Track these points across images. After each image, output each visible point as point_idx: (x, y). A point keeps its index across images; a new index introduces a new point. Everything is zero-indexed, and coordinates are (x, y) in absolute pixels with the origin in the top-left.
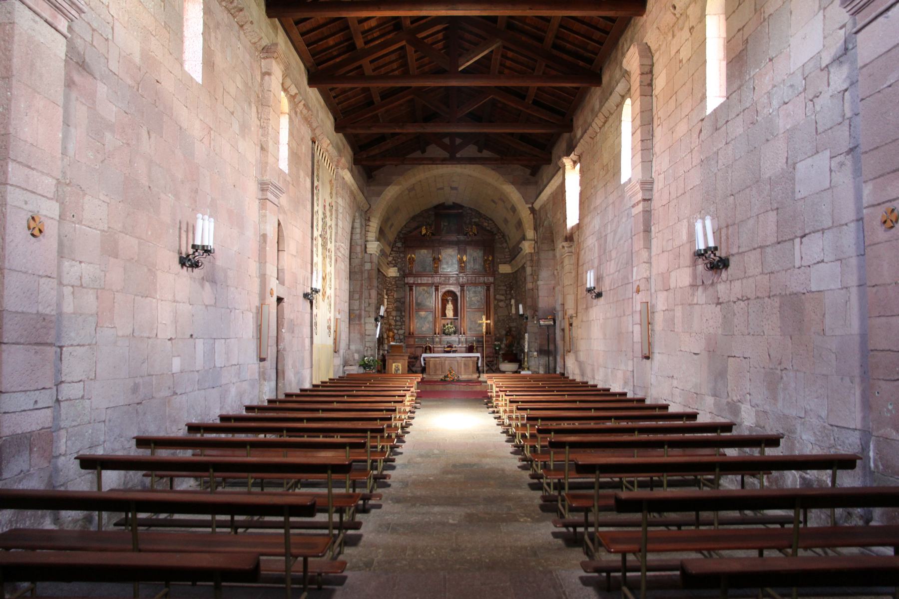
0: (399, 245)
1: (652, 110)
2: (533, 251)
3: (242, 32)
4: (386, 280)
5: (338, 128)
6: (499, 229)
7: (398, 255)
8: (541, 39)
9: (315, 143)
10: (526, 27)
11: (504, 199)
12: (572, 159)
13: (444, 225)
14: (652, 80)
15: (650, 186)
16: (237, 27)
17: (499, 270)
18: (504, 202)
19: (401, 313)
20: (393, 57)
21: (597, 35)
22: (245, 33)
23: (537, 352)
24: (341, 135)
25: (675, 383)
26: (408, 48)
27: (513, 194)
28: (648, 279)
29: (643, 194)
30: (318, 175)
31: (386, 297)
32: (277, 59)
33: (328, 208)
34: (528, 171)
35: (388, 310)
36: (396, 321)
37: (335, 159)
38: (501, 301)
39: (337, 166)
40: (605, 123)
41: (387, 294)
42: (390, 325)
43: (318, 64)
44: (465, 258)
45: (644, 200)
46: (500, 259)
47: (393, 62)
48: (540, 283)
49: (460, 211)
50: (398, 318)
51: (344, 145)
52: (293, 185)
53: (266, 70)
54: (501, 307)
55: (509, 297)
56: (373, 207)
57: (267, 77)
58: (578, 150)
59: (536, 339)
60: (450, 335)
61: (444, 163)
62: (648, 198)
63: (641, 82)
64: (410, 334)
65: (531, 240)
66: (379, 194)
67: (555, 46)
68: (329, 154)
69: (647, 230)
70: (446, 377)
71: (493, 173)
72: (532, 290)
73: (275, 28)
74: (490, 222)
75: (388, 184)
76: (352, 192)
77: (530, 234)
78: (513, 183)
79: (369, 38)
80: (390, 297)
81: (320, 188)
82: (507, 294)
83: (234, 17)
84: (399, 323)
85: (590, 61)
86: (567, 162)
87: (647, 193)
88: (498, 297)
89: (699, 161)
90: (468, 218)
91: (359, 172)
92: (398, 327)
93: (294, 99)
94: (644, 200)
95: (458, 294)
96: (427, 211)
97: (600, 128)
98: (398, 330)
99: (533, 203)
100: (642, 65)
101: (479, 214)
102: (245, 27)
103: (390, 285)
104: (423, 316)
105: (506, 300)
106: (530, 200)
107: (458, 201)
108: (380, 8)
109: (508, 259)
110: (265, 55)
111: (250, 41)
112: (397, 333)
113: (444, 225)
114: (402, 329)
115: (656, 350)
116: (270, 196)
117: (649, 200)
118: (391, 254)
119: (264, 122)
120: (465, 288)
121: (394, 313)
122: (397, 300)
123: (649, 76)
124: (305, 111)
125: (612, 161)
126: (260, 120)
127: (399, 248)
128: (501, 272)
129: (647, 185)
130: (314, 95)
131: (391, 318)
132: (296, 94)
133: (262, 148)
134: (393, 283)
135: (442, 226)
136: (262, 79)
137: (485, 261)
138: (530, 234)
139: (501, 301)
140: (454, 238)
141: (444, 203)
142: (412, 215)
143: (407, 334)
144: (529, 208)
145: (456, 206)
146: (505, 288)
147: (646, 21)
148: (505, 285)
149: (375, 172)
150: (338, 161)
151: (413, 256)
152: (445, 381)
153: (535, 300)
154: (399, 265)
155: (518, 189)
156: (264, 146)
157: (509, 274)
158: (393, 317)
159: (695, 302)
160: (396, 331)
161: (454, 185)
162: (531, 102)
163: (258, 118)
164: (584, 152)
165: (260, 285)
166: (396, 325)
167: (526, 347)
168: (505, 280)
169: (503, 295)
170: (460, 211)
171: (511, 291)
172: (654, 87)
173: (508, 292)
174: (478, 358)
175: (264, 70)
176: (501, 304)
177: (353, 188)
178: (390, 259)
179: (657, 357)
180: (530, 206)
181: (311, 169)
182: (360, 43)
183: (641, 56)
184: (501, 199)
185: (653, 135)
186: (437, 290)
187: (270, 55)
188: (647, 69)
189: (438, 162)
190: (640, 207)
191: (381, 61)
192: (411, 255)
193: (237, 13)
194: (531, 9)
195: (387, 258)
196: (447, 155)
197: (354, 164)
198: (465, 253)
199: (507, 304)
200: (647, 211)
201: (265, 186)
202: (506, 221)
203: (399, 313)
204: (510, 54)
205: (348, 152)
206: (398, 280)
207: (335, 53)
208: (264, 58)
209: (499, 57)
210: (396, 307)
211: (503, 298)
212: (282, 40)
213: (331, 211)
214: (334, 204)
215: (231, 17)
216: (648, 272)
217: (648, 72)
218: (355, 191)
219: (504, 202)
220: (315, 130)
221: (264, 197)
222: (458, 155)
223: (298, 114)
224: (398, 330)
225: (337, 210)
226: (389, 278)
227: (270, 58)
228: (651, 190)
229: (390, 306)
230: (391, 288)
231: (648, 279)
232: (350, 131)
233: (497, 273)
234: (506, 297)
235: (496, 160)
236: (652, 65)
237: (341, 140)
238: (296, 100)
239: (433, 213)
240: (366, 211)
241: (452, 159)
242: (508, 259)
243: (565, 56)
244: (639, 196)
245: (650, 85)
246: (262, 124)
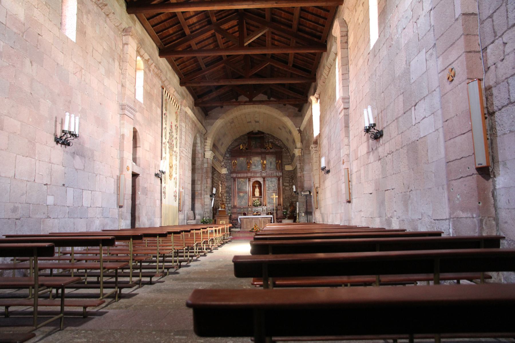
0: (228, 155)
1: (348, 57)
2: (300, 155)
3: (108, 19)
4: (221, 176)
5: (182, 84)
6: (284, 145)
7: (227, 161)
8: (290, 26)
9: (163, 89)
10: (282, 19)
11: (285, 127)
12: (316, 97)
13: (253, 144)
14: (347, 40)
15: (348, 100)
16: (104, 15)
17: (285, 169)
18: (285, 128)
19: (229, 195)
20: (210, 41)
21: (321, 21)
22: (110, 20)
23: (304, 213)
24: (184, 88)
25: (362, 214)
26: (217, 34)
27: (288, 122)
28: (348, 155)
29: (344, 105)
30: (166, 108)
31: (221, 185)
32: (133, 36)
33: (174, 127)
34: (297, 109)
35: (222, 193)
36: (226, 199)
37: (180, 101)
38: (287, 186)
39: (181, 105)
40: (329, 72)
41: (221, 184)
42: (223, 201)
43: (165, 45)
44: (265, 162)
45: (345, 108)
46: (286, 162)
47: (209, 44)
48: (305, 173)
49: (262, 135)
50: (228, 197)
51: (187, 95)
52: (147, 110)
53: (126, 42)
54: (286, 190)
55: (291, 184)
56: (209, 132)
57: (126, 46)
58: (318, 91)
59: (304, 205)
60: (257, 206)
61: (246, 104)
62: (346, 107)
63: (341, 41)
64: (234, 206)
65: (299, 148)
66: (212, 124)
67: (299, 30)
68: (175, 97)
69: (347, 126)
70: (253, 229)
71: (277, 110)
72: (301, 177)
73: (133, 20)
74: (279, 141)
75: (217, 119)
76: (193, 122)
77: (299, 145)
78: (288, 116)
79: (194, 29)
80: (223, 185)
81: (168, 114)
83: (102, 9)
84: (228, 200)
85: (319, 37)
86: (313, 99)
87: (346, 104)
88: (285, 184)
89: (368, 78)
90: (267, 139)
91: (198, 111)
92: (228, 203)
93: (148, 62)
94: (345, 108)
95: (262, 183)
96: (243, 136)
97: (327, 76)
98: (228, 204)
99: (300, 127)
100: (341, 31)
101: (273, 137)
102: (110, 16)
104: (242, 196)
105: (290, 185)
106: (298, 125)
107: (261, 130)
108: (190, 6)
110: (125, 34)
111: (114, 25)
112: (227, 206)
113: (253, 144)
114: (230, 204)
115: (354, 196)
116: (126, 112)
117: (348, 108)
118: (223, 161)
119: (124, 71)
120: (266, 179)
121: (225, 195)
122: (226, 187)
123: (346, 38)
124: (156, 70)
125: (333, 93)
126: (121, 70)
127: (228, 157)
129: (346, 100)
130: (163, 62)
131: (224, 197)
132: (149, 59)
133: (123, 86)
134: (225, 177)
136: (123, 47)
137: (277, 163)
138: (299, 145)
139: (287, 186)
140: (259, 150)
141: (253, 131)
142: (235, 138)
143: (233, 206)
144: (298, 130)
145: (260, 132)
146: (289, 179)
147: (344, 7)
148: (289, 177)
149: (210, 112)
150: (182, 102)
151: (236, 161)
152: (252, 231)
153: (302, 183)
154: (228, 167)
155: (291, 119)
156: (124, 85)
158: (225, 197)
159: (369, 162)
160: (226, 205)
161: (257, 119)
162: (291, 66)
163: (120, 68)
164: (321, 92)
165: (120, 164)
166: (227, 202)
167: (298, 210)
169: (288, 183)
170: (262, 135)
171: (292, 180)
172: (348, 43)
174: (271, 218)
175: (124, 42)
176: (287, 188)
177: (194, 119)
178: (223, 163)
179: (354, 201)
180: (298, 129)
181: (161, 104)
182: (187, 31)
183: (341, 27)
184: (283, 127)
185: (349, 71)
186: (249, 180)
187: (128, 33)
188: (344, 34)
189: (242, 104)
190: (343, 114)
191: (203, 44)
193: (103, 7)
194: (276, 3)
195: (221, 163)
196: (248, 100)
197: (195, 106)
198: (265, 158)
199: (290, 188)
200: (347, 115)
201: (123, 107)
202: (287, 139)
203: (228, 195)
204: (276, 37)
205: (190, 99)
207: (174, 38)
208: (124, 35)
209: (270, 39)
210: (226, 191)
211: (288, 184)
212: (138, 28)
213: (176, 129)
214: (178, 125)
215: (100, 9)
216: (348, 150)
217: (345, 35)
218: (195, 121)
219: (285, 128)
220: (164, 82)
221: (123, 113)
222: (254, 99)
223: (151, 71)
224: (228, 204)
225: (181, 130)
226: (222, 174)
227: (128, 35)
228: (349, 103)
229: (223, 191)
231: (348, 155)
232: (188, 85)
233: (284, 170)
234: (289, 184)
235: (275, 102)
236: (348, 31)
237: (185, 91)
238: (149, 63)
239: (247, 137)
240: (205, 134)
241: (251, 102)
243: (306, 36)
244: (342, 107)
245: (347, 42)
246: (123, 72)
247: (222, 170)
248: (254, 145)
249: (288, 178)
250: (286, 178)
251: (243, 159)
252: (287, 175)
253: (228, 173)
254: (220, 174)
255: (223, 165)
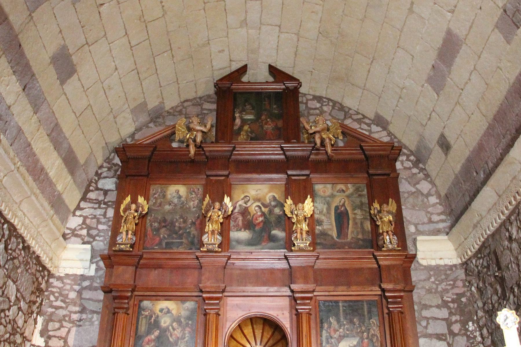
13: (244, 122)
17: (419, 256)
82: (452, 333)
103: (59, 303)
109: (441, 225)
113: (244, 122)
128: (424, 263)
135: (238, 121)
146: (444, 313)
148: (445, 304)
151: (141, 200)
157: (452, 267)
168: (443, 286)
173: (456, 328)
178: (74, 222)
192: (134, 201)
195: (64, 220)
206: (90, 288)
230: (61, 312)
242: (441, 225)
247: (65, 254)
248: (246, 128)
249: (438, 307)
250: (426, 307)
251: (182, 190)
252: (429, 291)
253: (92, 273)
254: (50, 275)
255: (74, 233)
